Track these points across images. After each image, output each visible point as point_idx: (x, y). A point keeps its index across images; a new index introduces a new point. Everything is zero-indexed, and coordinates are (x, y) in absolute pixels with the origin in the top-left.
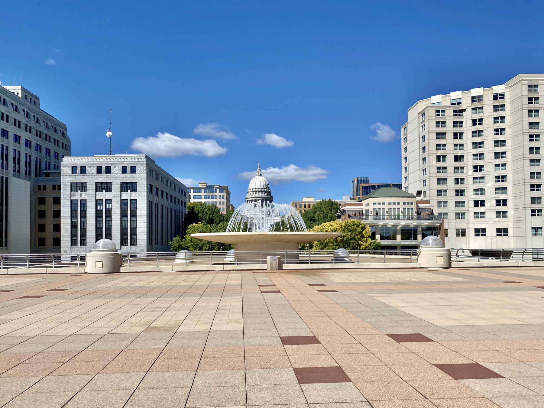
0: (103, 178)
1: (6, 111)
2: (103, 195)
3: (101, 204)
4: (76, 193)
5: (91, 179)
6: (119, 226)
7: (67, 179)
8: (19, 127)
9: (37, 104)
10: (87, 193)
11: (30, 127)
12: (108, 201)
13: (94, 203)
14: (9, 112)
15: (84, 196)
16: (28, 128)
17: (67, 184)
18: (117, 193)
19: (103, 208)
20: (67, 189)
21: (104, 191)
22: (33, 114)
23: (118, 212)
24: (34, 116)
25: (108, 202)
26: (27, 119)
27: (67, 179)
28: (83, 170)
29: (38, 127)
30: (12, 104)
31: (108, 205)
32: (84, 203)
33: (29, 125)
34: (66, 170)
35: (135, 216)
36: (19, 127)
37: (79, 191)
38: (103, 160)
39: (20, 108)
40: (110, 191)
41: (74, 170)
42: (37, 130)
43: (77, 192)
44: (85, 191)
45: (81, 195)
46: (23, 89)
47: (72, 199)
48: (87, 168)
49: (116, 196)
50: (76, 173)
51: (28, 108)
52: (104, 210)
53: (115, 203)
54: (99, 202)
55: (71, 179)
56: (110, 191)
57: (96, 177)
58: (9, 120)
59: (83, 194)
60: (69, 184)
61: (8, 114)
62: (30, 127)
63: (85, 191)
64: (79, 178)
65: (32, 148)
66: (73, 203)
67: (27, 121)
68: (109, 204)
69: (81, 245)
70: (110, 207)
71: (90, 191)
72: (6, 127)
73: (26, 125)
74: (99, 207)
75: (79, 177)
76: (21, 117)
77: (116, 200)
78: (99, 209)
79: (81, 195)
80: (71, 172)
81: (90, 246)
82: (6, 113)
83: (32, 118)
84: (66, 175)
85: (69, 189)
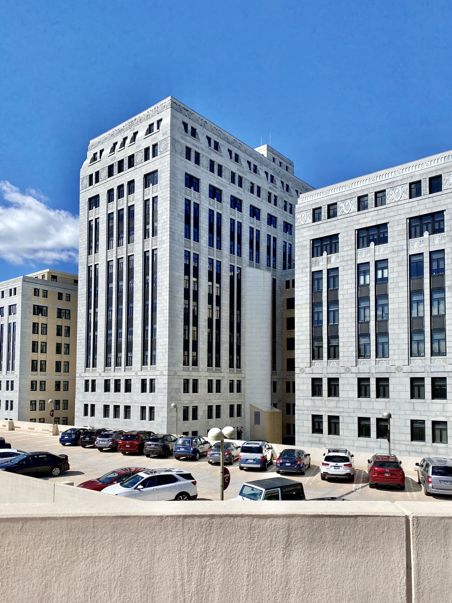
0: (370, 218)
1: (238, 170)
2: (371, 253)
3: (366, 272)
4: (320, 258)
5: (345, 227)
6: (405, 315)
7: (305, 233)
8: (259, 195)
9: (290, 170)
10: (341, 253)
11: (275, 197)
12: (381, 264)
13: (352, 272)
14: (242, 172)
15: (335, 260)
16: (273, 198)
17: (304, 243)
18: (400, 243)
19: (370, 279)
20: (305, 253)
21: (372, 244)
22: (280, 179)
23: (401, 284)
24: (282, 183)
25: (380, 266)
26: (271, 185)
27: (305, 234)
28: (332, 210)
29: (287, 198)
30: (249, 163)
31: (380, 272)
32: (333, 274)
33: (273, 193)
34: (302, 218)
35: (442, 289)
36: (259, 195)
37: (325, 253)
38: (366, 184)
39: (261, 170)
40: (384, 240)
41: (316, 215)
42: (286, 202)
43: (322, 255)
44: (336, 251)
45: (328, 260)
46: (269, 149)
47: (314, 269)
48: (340, 205)
49: (397, 250)
50: (319, 219)
51: (274, 169)
52: (372, 284)
53: (395, 265)
54: (361, 269)
55: (311, 232)
56: (384, 240)
57: (355, 218)
58: (243, 184)
59: (333, 256)
60: (308, 244)
61: (241, 175)
62: (275, 197)
63: (336, 251)
64: (325, 228)
65: (278, 227)
66: (315, 277)
67: (270, 188)
68: (382, 269)
69: (329, 357)
70: (385, 276)
71: (345, 249)
72: (238, 193)
73: (270, 193)
74: (362, 278)
75: (325, 225)
76: (261, 181)
77: (396, 259)
78: (362, 282)
79: (328, 260)
80: (311, 220)
81: (346, 359)
82: (238, 173)
83: (279, 184)
84: (304, 226)
85: (308, 252)
